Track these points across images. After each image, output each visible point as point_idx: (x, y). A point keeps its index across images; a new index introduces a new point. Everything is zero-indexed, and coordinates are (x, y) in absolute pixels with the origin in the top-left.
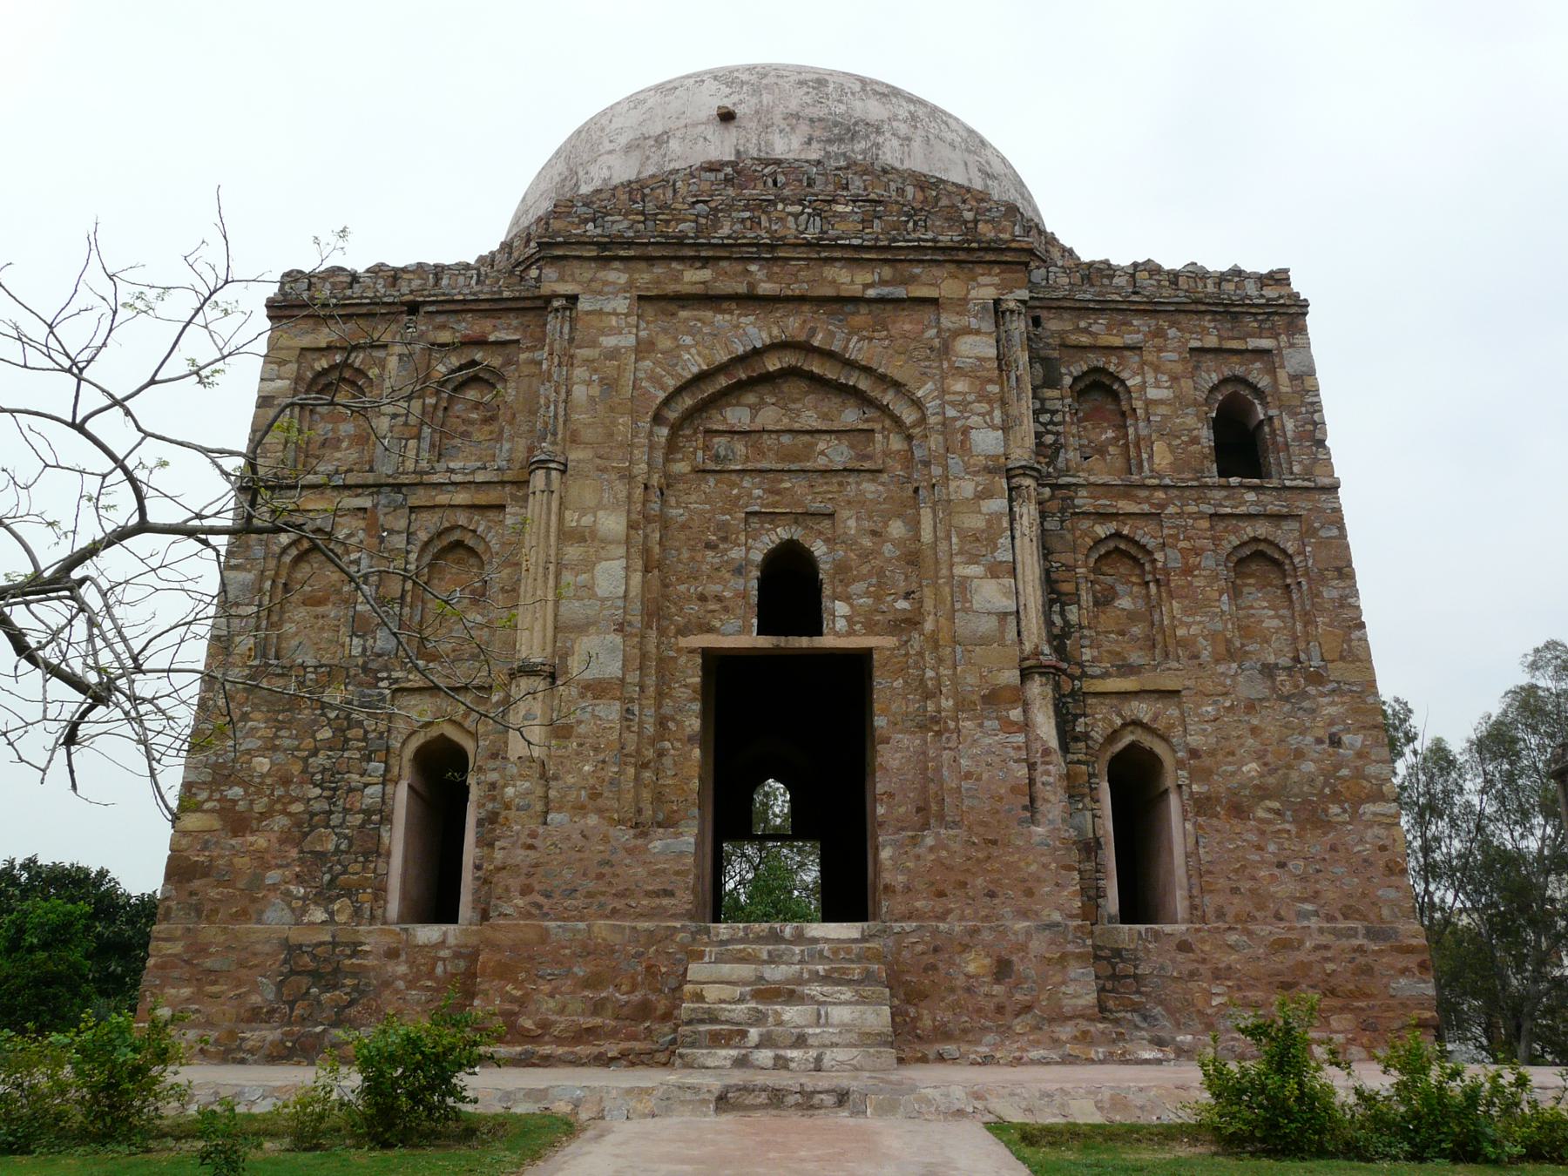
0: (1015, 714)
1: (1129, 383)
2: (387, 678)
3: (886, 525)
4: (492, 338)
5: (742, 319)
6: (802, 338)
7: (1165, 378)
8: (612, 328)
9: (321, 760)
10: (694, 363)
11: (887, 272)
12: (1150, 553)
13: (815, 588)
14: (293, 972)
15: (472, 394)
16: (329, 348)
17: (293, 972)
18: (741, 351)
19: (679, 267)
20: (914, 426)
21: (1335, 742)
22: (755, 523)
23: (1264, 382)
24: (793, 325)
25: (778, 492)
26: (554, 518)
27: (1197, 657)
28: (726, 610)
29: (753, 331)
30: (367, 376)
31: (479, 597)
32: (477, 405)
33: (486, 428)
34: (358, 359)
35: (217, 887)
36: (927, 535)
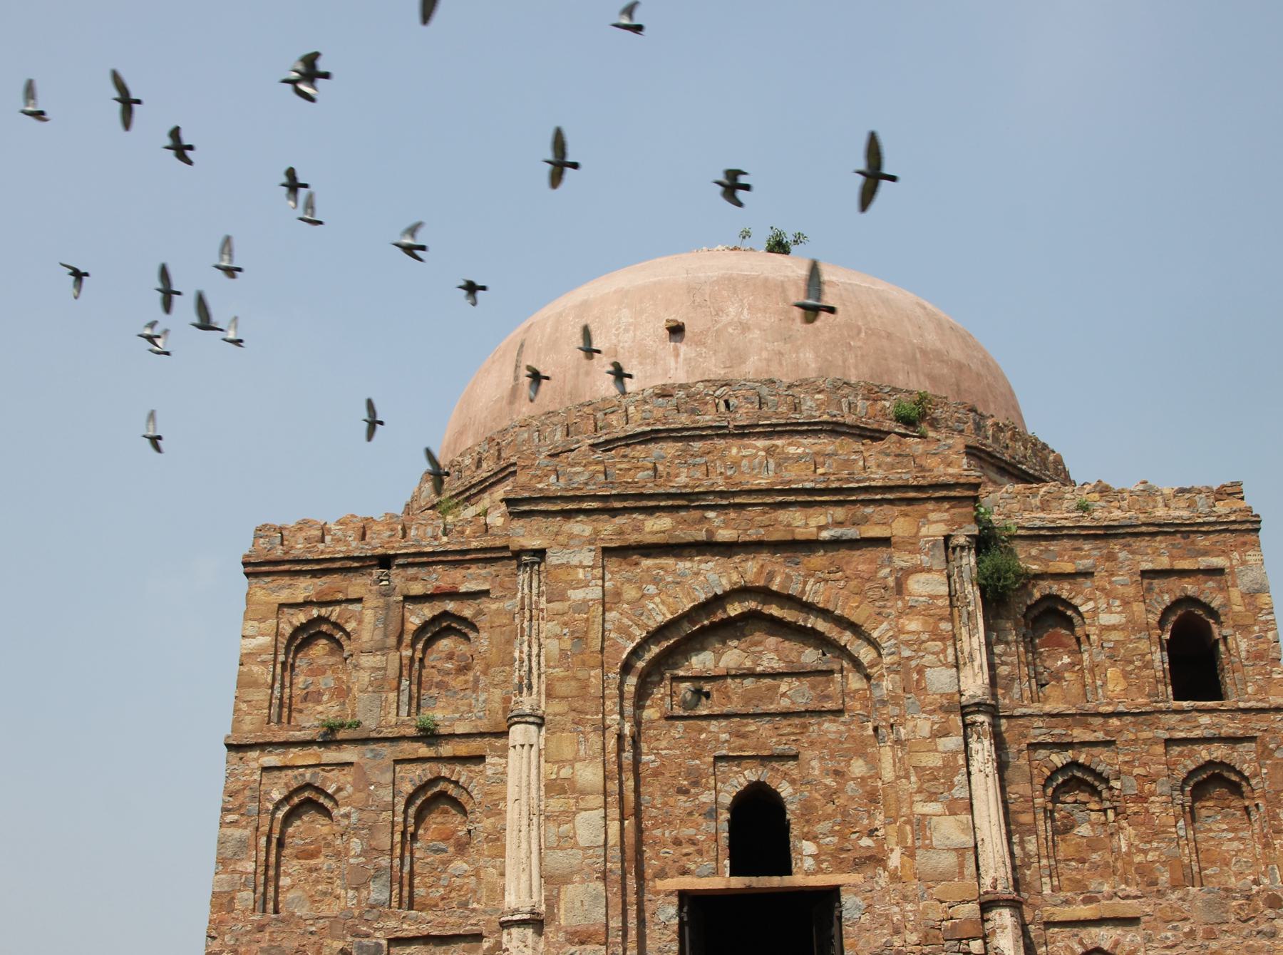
1: (1082, 609)
3: (848, 765)
4: (462, 589)
5: (703, 566)
6: (762, 583)
7: (1118, 603)
8: (579, 581)
10: (662, 615)
11: (840, 513)
12: (1106, 781)
13: (785, 828)
15: (445, 644)
16: (307, 603)
18: (702, 597)
19: (641, 517)
20: (872, 666)
22: (723, 767)
24: (750, 569)
25: (744, 736)
26: (534, 771)
27: (1154, 883)
28: (700, 852)
29: (712, 576)
30: (344, 630)
31: (462, 848)
32: (450, 657)
33: (462, 678)
34: (335, 613)
36: (888, 773)
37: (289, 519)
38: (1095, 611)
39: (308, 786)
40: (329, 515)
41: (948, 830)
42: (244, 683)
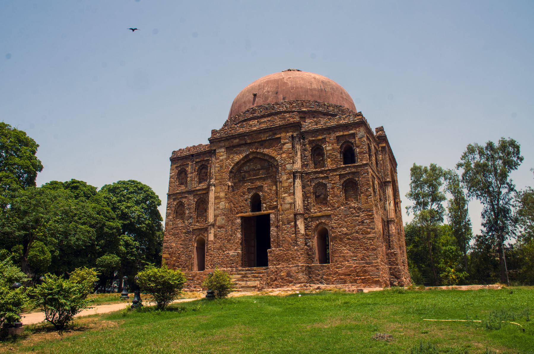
0: (293, 223)
11: (271, 133)
15: (203, 171)
21: (363, 222)
23: (353, 141)
37: (177, 149)
38: (326, 147)
40: (183, 147)
41: (289, 199)
42: (170, 183)
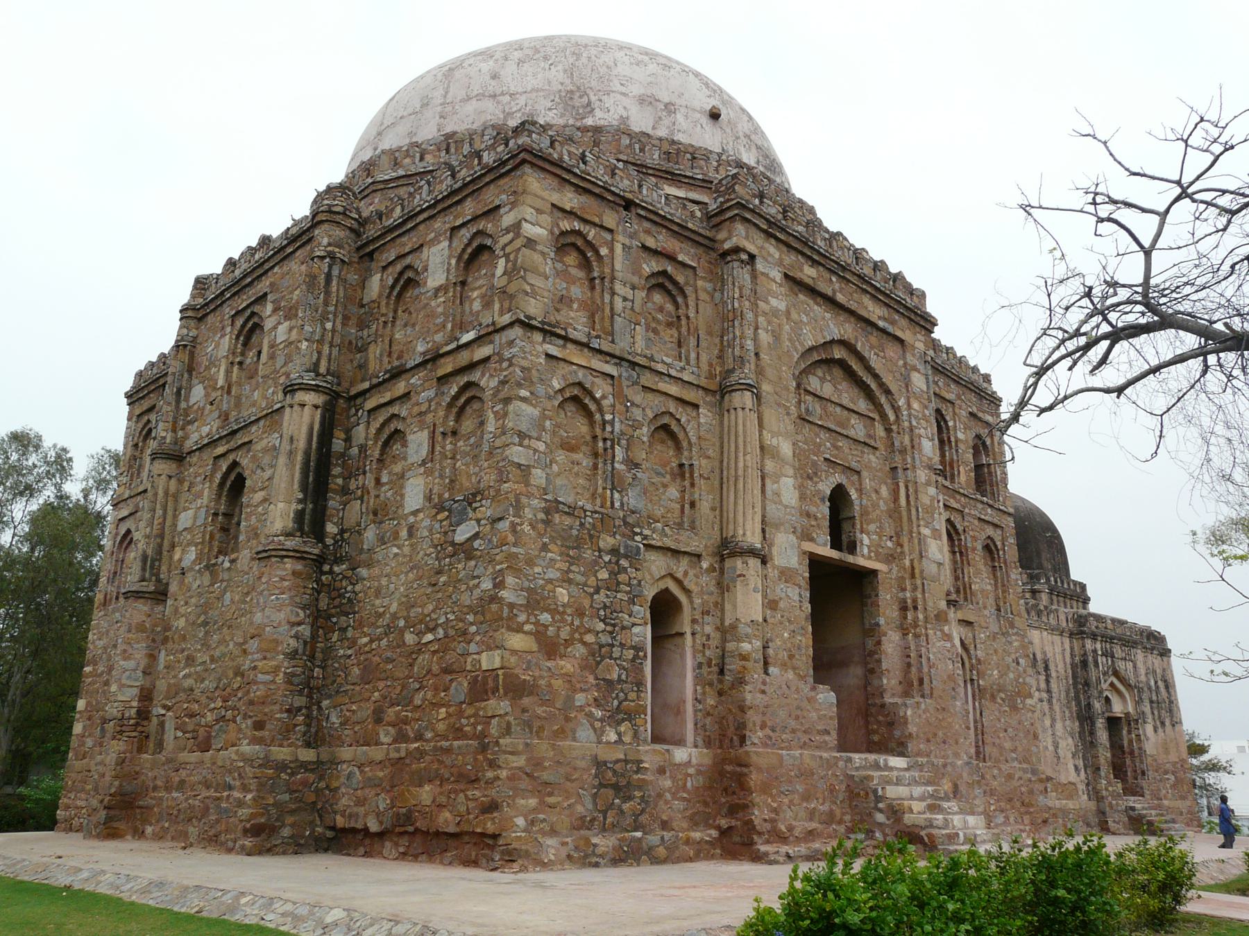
2: (641, 534)
4: (680, 258)
9: (601, 597)
14: (601, 785)
17: (601, 785)
34: (592, 233)
35: (542, 705)
39: (580, 384)
